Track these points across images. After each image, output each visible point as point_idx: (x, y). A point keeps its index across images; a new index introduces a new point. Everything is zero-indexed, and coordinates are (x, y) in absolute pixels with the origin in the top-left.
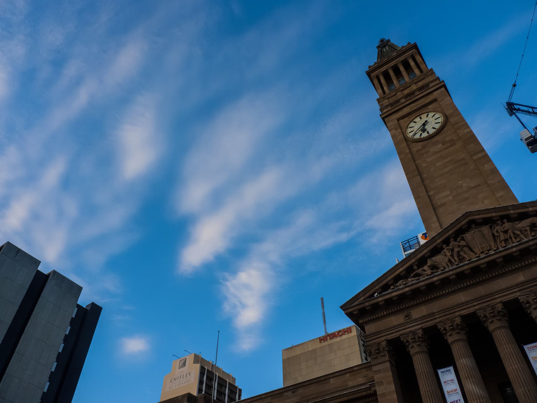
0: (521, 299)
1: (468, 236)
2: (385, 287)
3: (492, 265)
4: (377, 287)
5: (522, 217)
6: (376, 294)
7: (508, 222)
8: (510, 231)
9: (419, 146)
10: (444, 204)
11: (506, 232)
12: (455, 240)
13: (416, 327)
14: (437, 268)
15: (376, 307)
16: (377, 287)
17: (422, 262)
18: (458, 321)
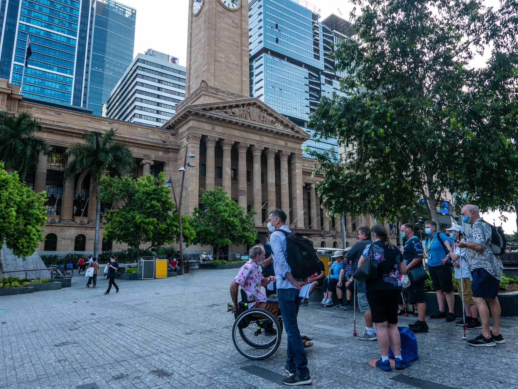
0: (256, 146)
2: (211, 109)
5: (271, 115)
9: (220, 9)
10: (219, 61)
11: (264, 117)
13: (217, 137)
15: (204, 115)
17: (231, 107)
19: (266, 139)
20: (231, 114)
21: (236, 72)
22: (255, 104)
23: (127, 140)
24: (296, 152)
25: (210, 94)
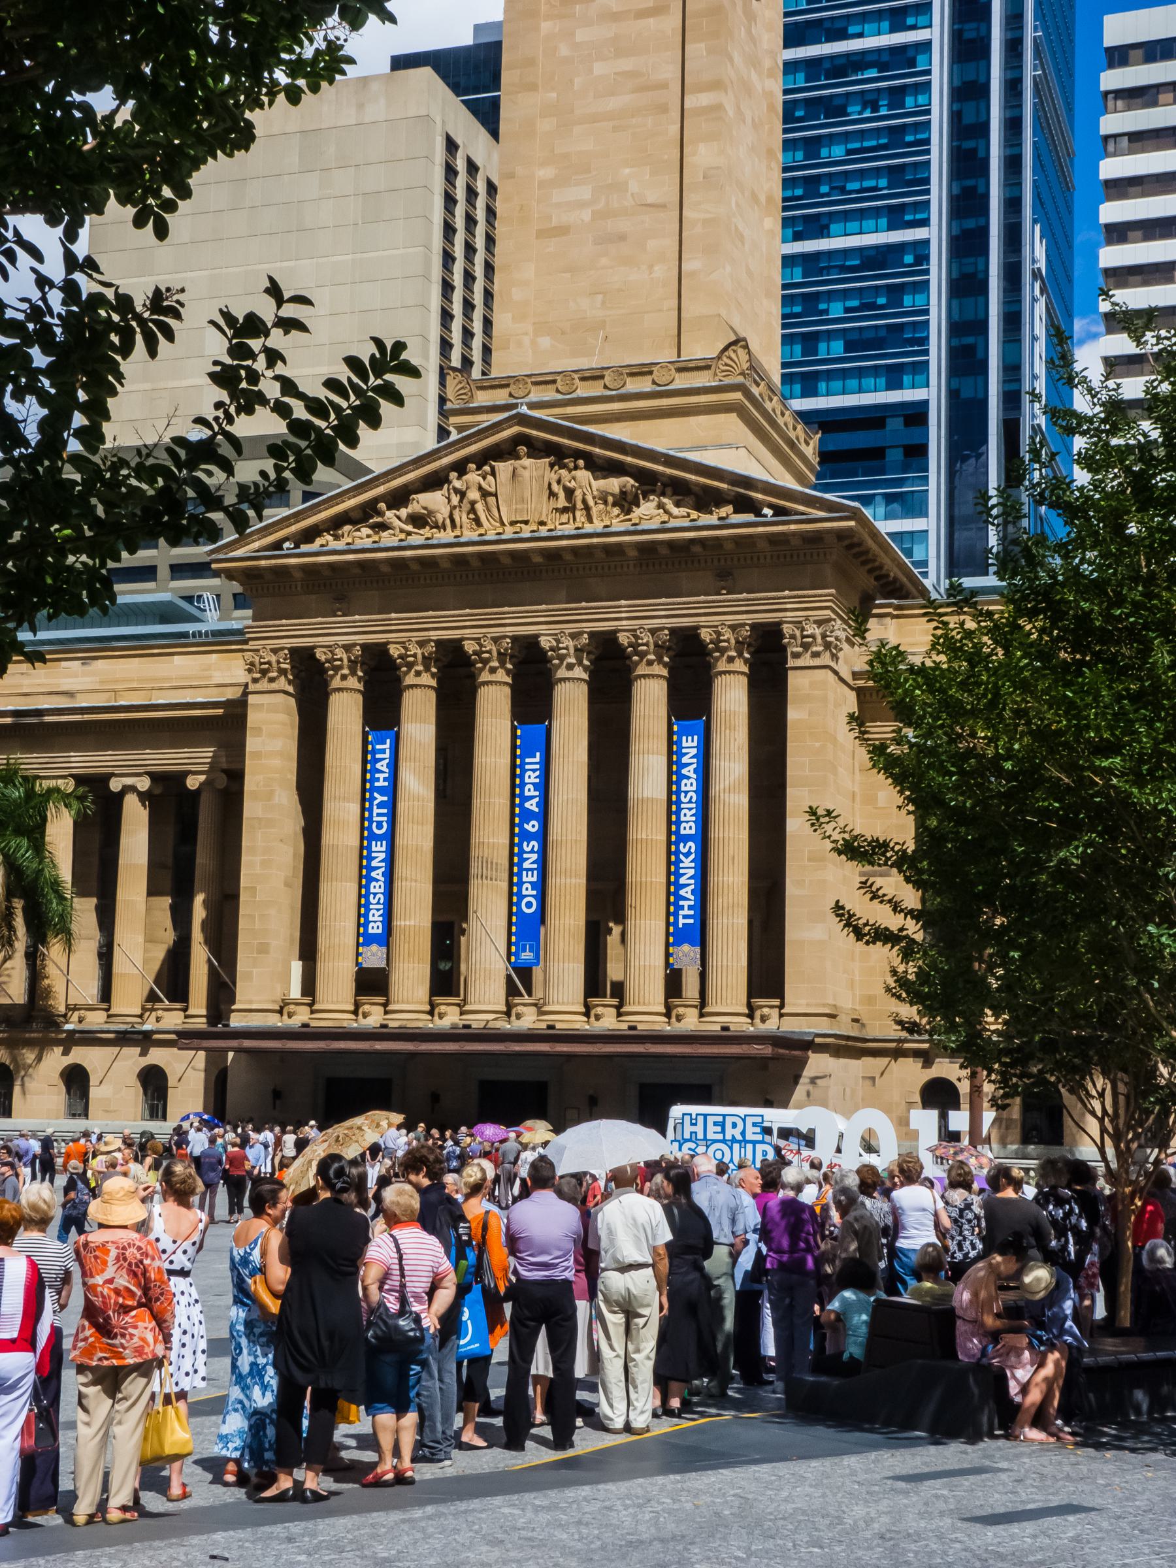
0: (545, 642)
1: (504, 468)
2: (309, 535)
4: (293, 529)
6: (286, 545)
7: (587, 468)
8: (578, 494)
10: (562, 231)
11: (569, 493)
12: (478, 469)
14: (427, 523)
15: (282, 573)
17: (399, 498)
21: (652, 244)
23: (122, 716)
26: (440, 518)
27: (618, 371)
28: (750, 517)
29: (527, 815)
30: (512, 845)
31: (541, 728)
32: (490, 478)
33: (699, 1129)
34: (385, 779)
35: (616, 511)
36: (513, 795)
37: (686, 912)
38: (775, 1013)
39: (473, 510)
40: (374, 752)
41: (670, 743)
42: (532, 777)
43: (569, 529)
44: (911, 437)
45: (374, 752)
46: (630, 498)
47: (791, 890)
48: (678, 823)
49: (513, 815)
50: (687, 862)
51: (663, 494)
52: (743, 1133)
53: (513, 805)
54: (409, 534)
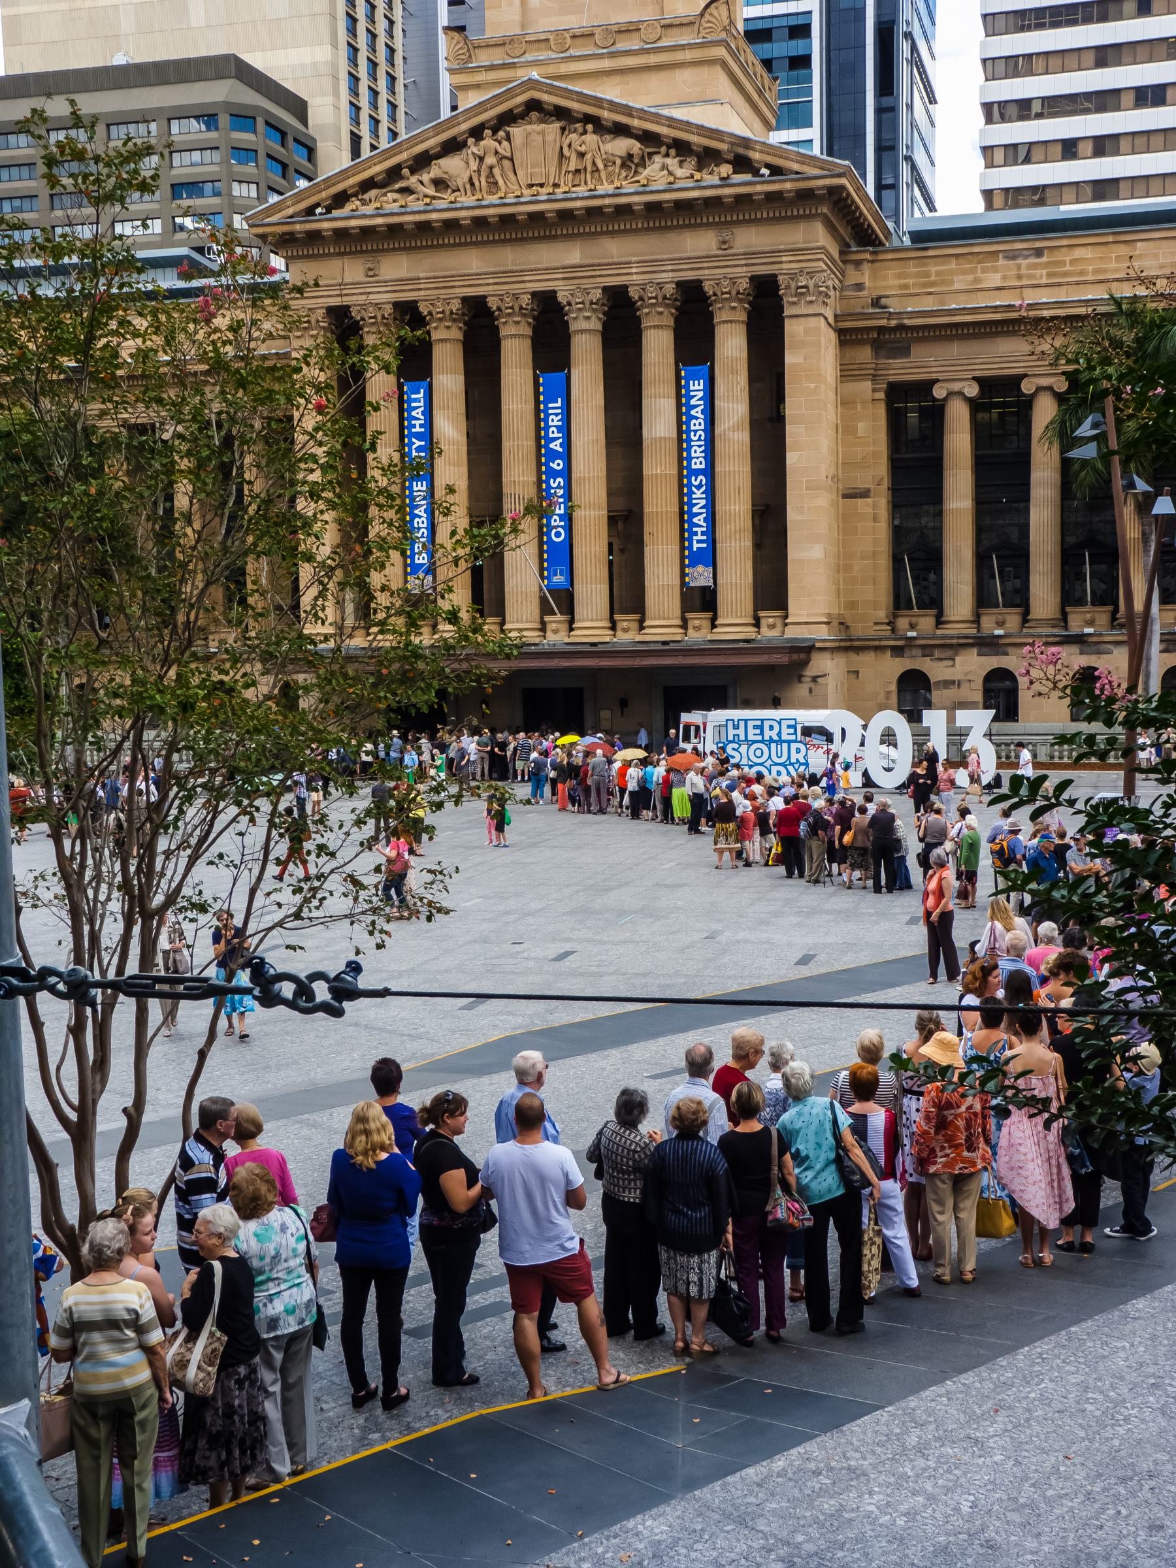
0: (562, 297)
1: (517, 131)
2: (340, 199)
3: (536, 218)
4: (324, 194)
6: (319, 210)
8: (588, 156)
13: (384, 297)
15: (314, 237)
16: (324, 194)
17: (422, 161)
18: (456, 305)
19: (613, 249)
20: (431, 191)
22: (534, 106)
24: (785, 267)
25: (480, 77)
26: (460, 183)
27: (607, 29)
28: (747, 177)
29: (553, 455)
30: (539, 481)
31: (562, 375)
32: (505, 143)
33: (741, 732)
34: (421, 426)
35: (624, 174)
36: (538, 438)
37: (700, 537)
38: (779, 622)
39: (491, 174)
40: (410, 401)
41: (678, 387)
42: (555, 421)
43: (581, 191)
44: (795, 48)
45: (410, 401)
46: (636, 161)
47: (792, 515)
48: (689, 459)
49: (539, 455)
50: (698, 494)
51: (667, 155)
52: (779, 734)
53: (539, 447)
54: (434, 198)
